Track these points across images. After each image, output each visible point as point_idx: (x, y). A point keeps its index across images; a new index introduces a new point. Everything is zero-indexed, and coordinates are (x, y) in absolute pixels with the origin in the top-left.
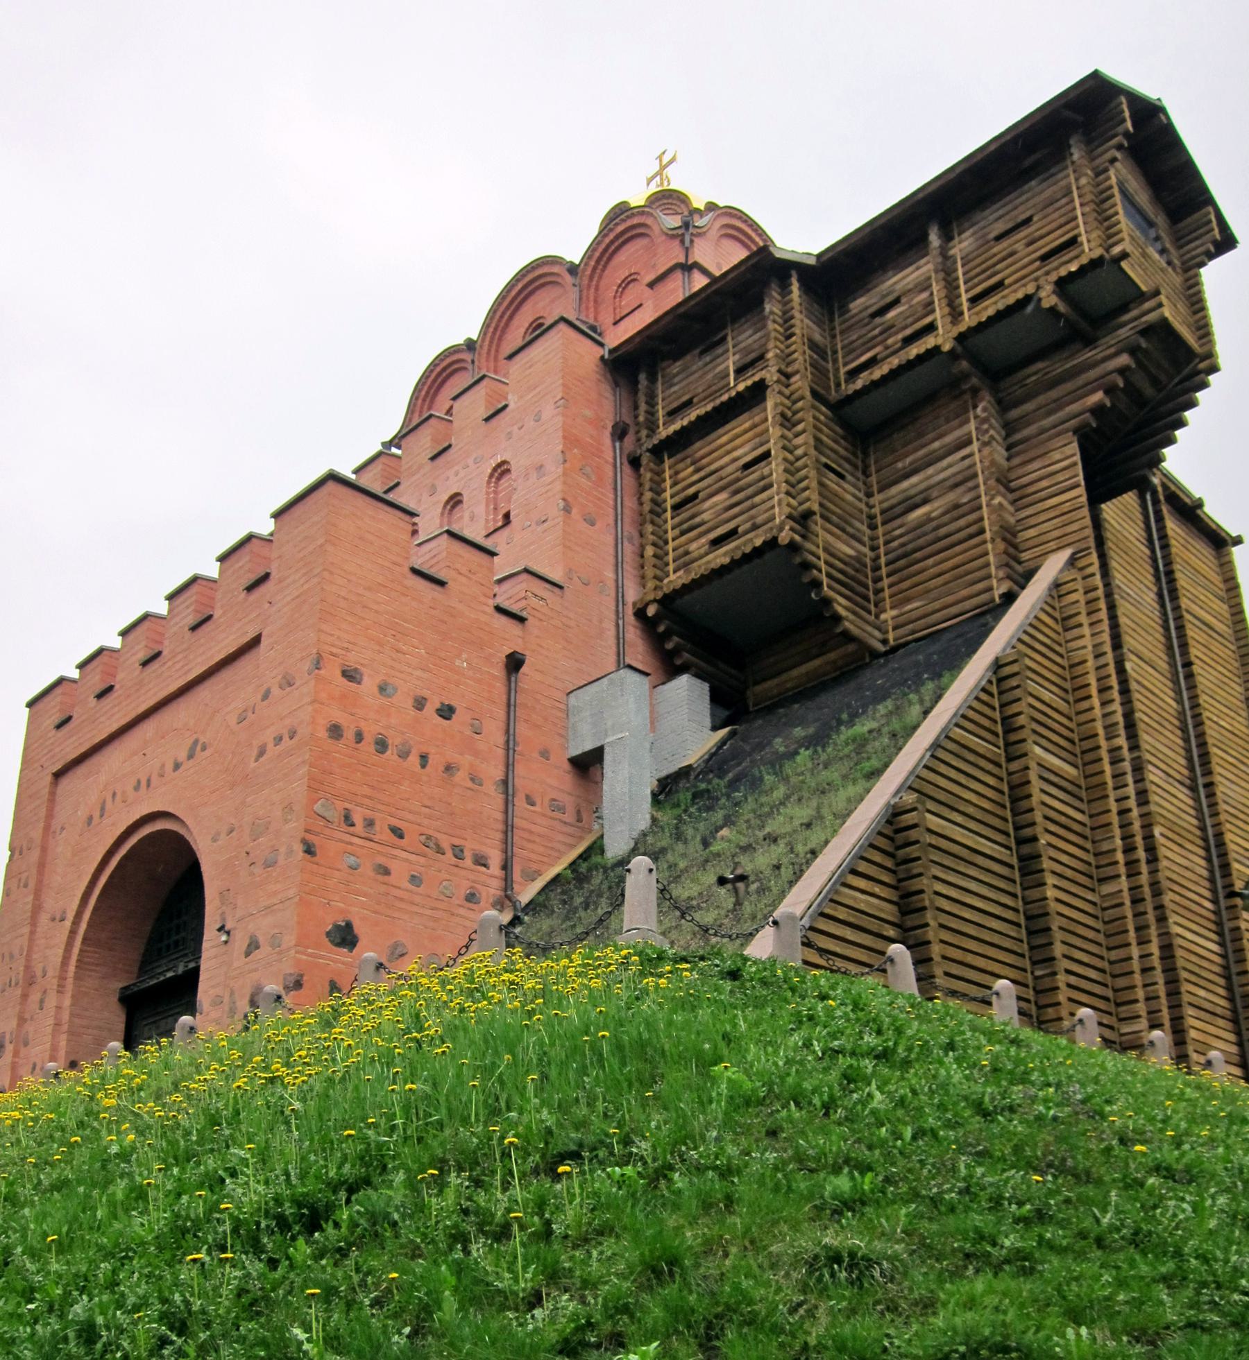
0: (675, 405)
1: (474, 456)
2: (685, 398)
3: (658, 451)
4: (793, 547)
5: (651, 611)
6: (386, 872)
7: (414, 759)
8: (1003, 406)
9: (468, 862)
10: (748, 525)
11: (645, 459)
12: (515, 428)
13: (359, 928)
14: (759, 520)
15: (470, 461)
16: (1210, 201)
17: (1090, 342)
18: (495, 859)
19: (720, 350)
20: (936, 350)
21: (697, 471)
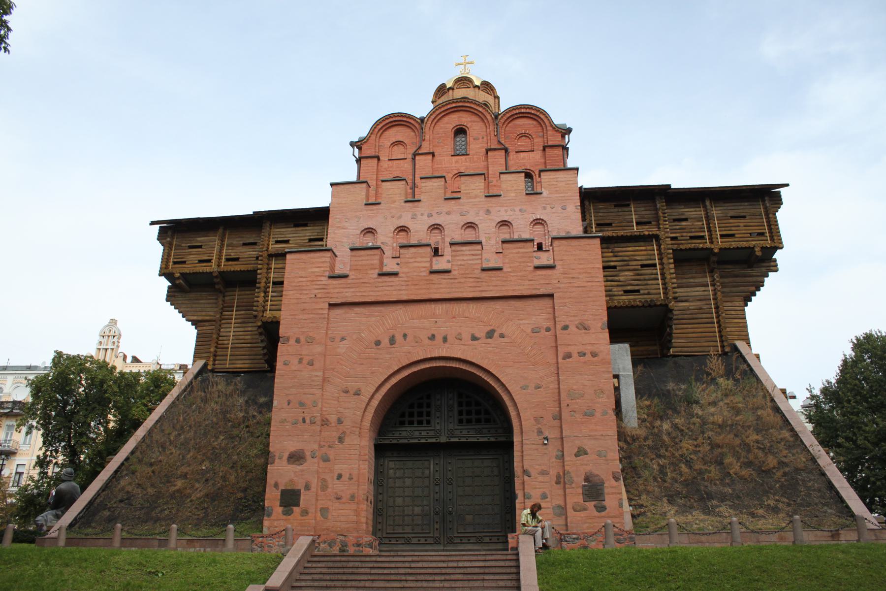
0: (602, 222)
10: (646, 292)
12: (548, 206)
14: (652, 291)
15: (517, 209)
19: (626, 209)
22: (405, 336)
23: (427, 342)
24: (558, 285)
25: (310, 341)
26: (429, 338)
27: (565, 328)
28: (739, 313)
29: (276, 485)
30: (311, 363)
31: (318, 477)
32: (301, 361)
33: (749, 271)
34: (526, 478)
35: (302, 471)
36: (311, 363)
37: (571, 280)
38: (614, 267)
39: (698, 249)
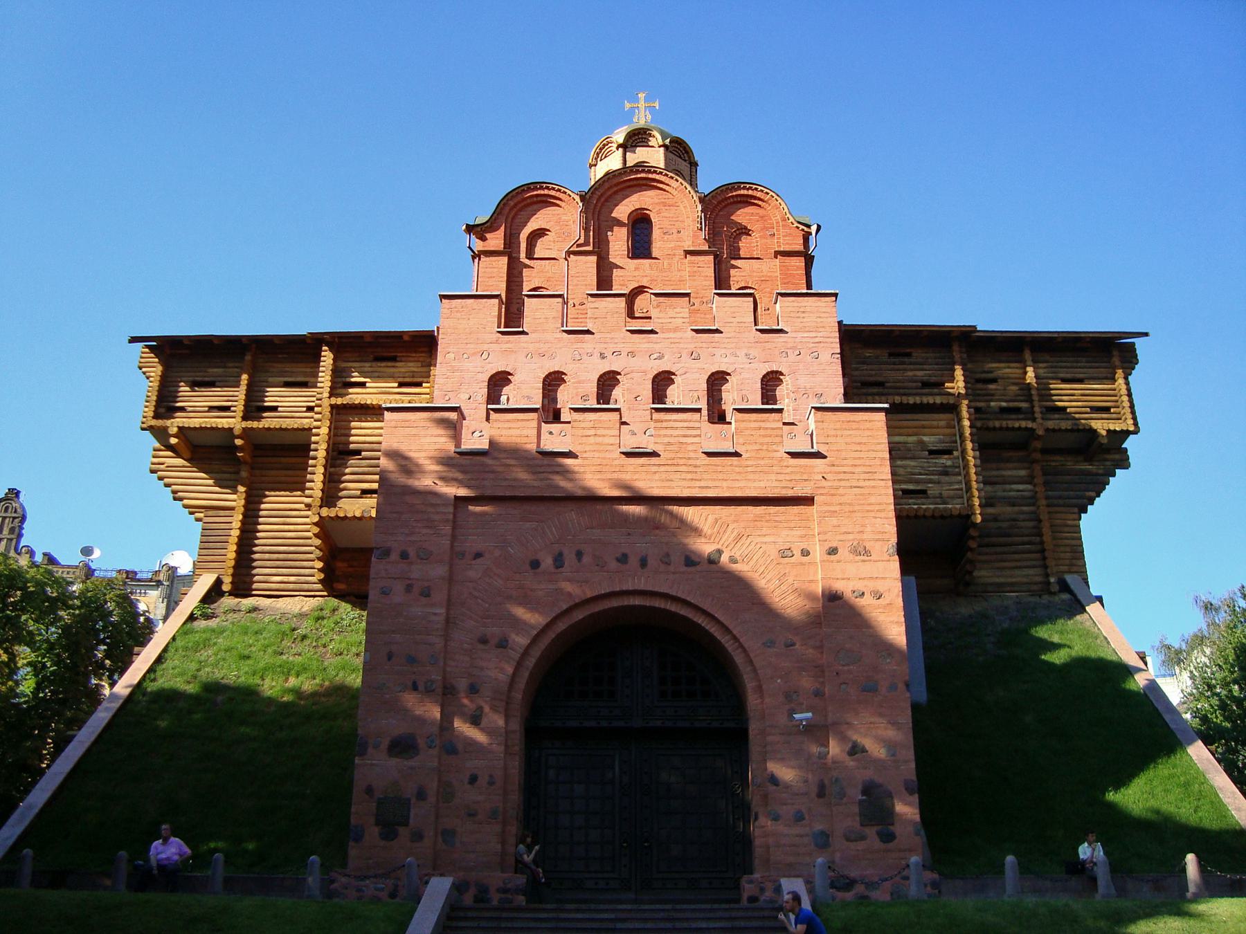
1: (745, 351)
2: (880, 379)
15: (741, 353)
20: (1032, 430)
22: (579, 554)
23: (613, 565)
24: (824, 483)
25: (425, 556)
26: (618, 560)
27: (833, 551)
28: (1072, 529)
29: (369, 790)
30: (426, 593)
31: (439, 781)
32: (409, 588)
34: (772, 788)
35: (412, 768)
36: (426, 593)
37: (842, 476)
39: (1013, 429)
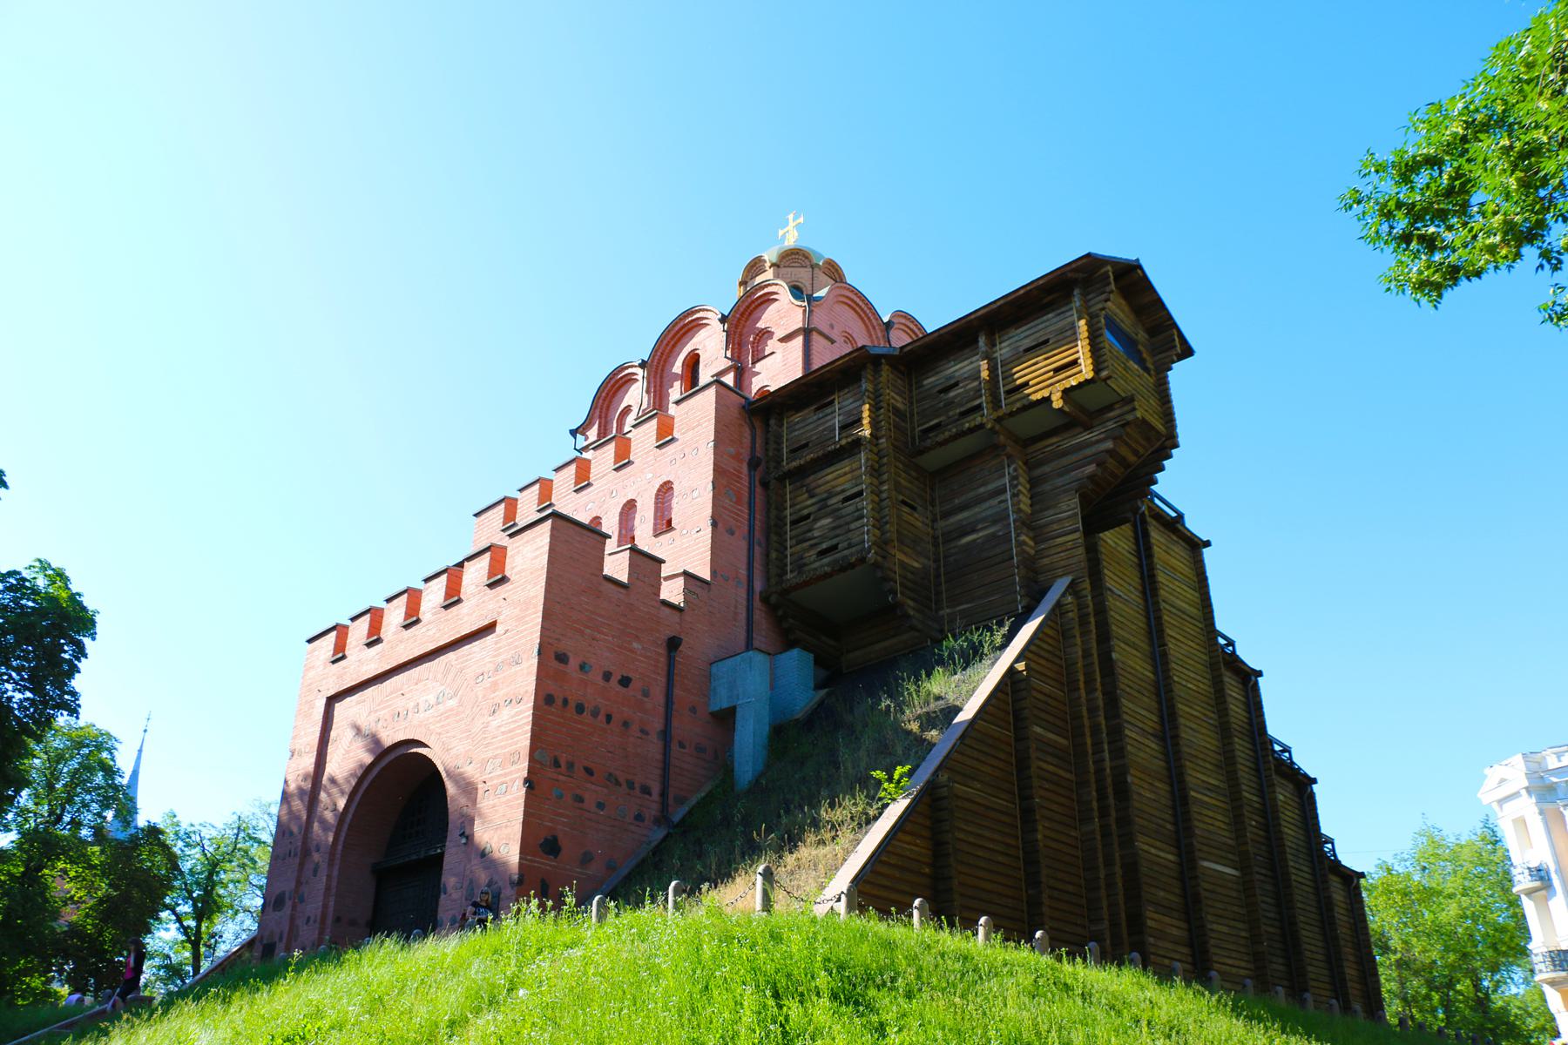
3: (781, 479)
4: (876, 565)
5: (773, 599)
6: (580, 800)
7: (602, 717)
8: (1030, 466)
9: (637, 790)
11: (773, 484)
13: (564, 842)
16: (1175, 325)
17: (1088, 428)
18: (656, 789)
20: (981, 426)
21: (812, 497)
33: (1086, 436)
38: (807, 517)
